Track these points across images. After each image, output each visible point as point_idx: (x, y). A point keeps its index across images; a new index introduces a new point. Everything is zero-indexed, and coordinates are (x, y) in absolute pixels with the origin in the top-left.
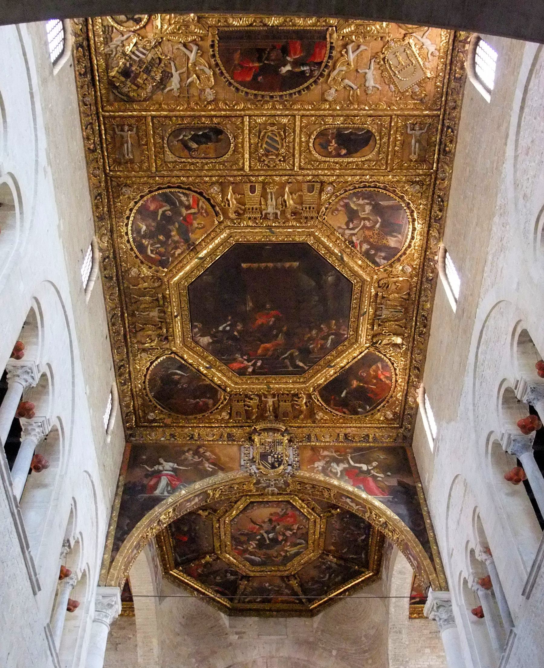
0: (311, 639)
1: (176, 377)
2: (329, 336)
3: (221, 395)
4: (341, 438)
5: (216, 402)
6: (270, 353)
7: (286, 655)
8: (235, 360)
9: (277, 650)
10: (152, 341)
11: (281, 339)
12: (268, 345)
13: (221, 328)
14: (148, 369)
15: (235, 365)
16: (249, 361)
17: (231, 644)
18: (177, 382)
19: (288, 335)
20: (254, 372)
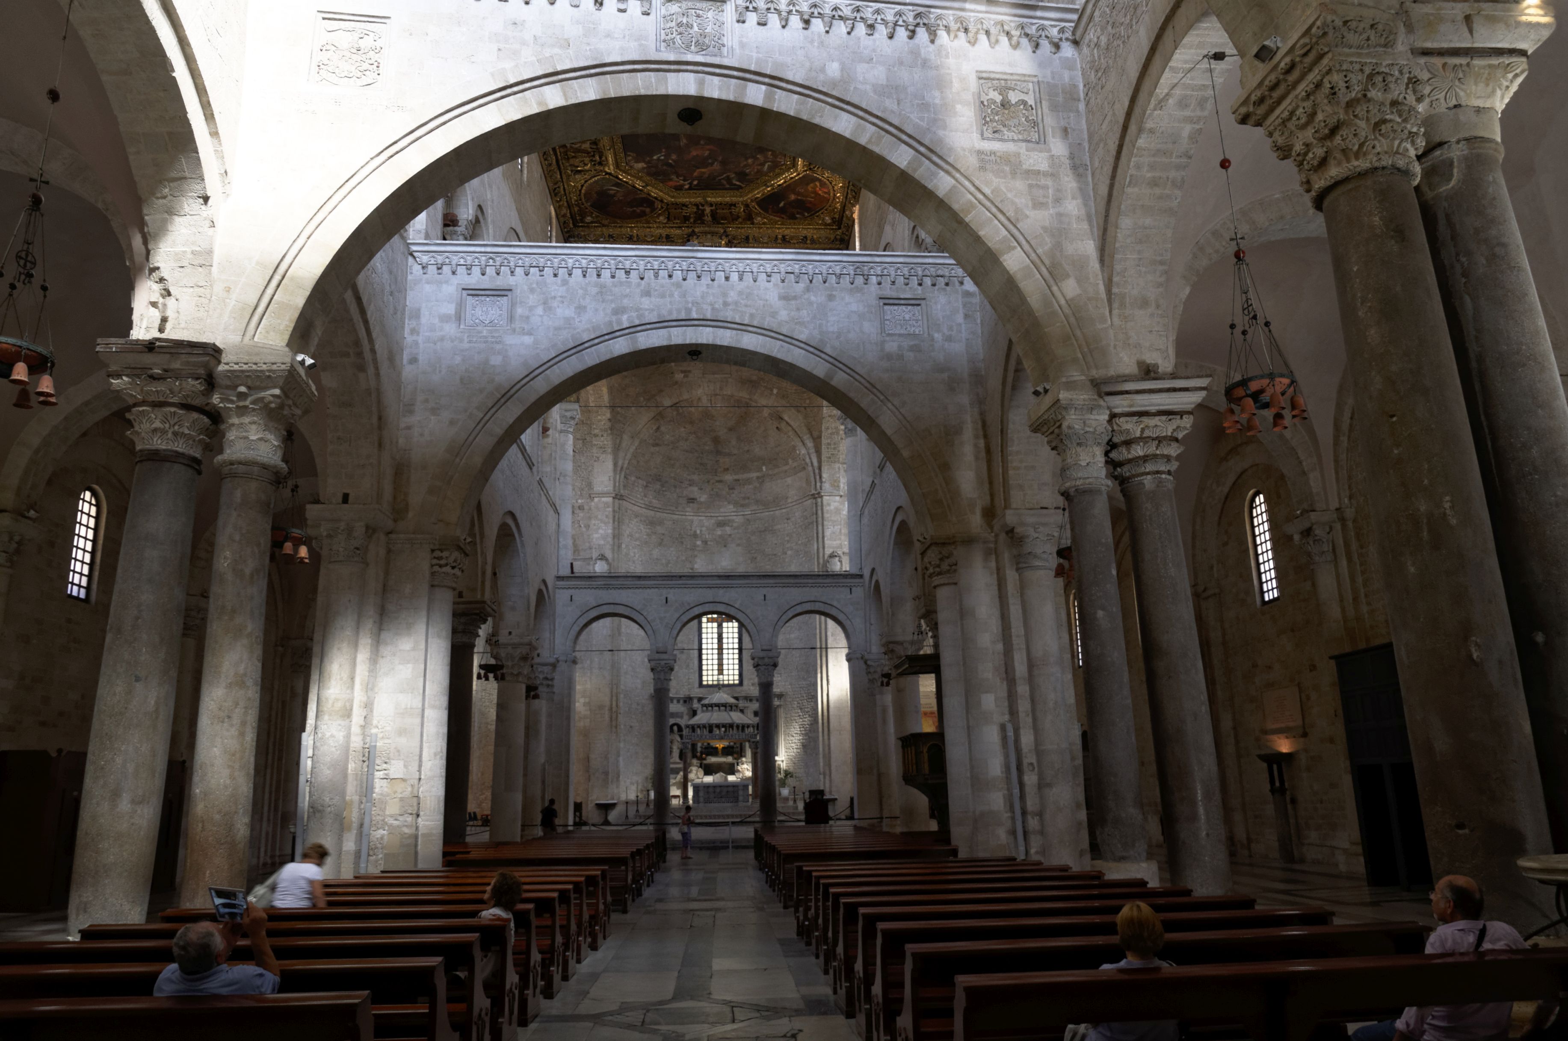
0: (754, 378)
1: (612, 192)
2: (765, 162)
3: (658, 205)
4: (779, 241)
5: (653, 209)
6: (707, 175)
7: (729, 393)
8: (671, 180)
9: (721, 389)
10: (586, 165)
11: (716, 166)
12: (703, 170)
13: (655, 157)
14: (582, 186)
15: (671, 183)
16: (684, 180)
17: (676, 383)
18: (614, 196)
19: (724, 163)
20: (690, 189)
